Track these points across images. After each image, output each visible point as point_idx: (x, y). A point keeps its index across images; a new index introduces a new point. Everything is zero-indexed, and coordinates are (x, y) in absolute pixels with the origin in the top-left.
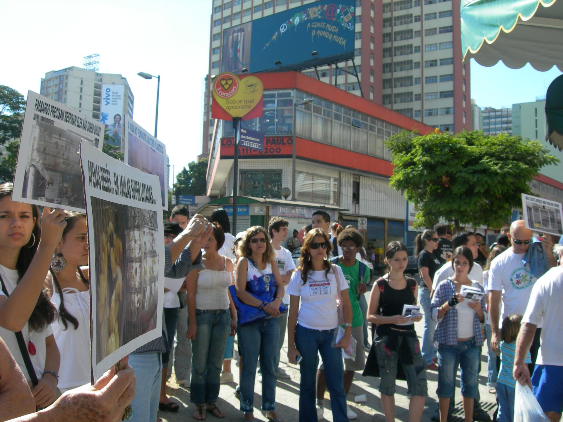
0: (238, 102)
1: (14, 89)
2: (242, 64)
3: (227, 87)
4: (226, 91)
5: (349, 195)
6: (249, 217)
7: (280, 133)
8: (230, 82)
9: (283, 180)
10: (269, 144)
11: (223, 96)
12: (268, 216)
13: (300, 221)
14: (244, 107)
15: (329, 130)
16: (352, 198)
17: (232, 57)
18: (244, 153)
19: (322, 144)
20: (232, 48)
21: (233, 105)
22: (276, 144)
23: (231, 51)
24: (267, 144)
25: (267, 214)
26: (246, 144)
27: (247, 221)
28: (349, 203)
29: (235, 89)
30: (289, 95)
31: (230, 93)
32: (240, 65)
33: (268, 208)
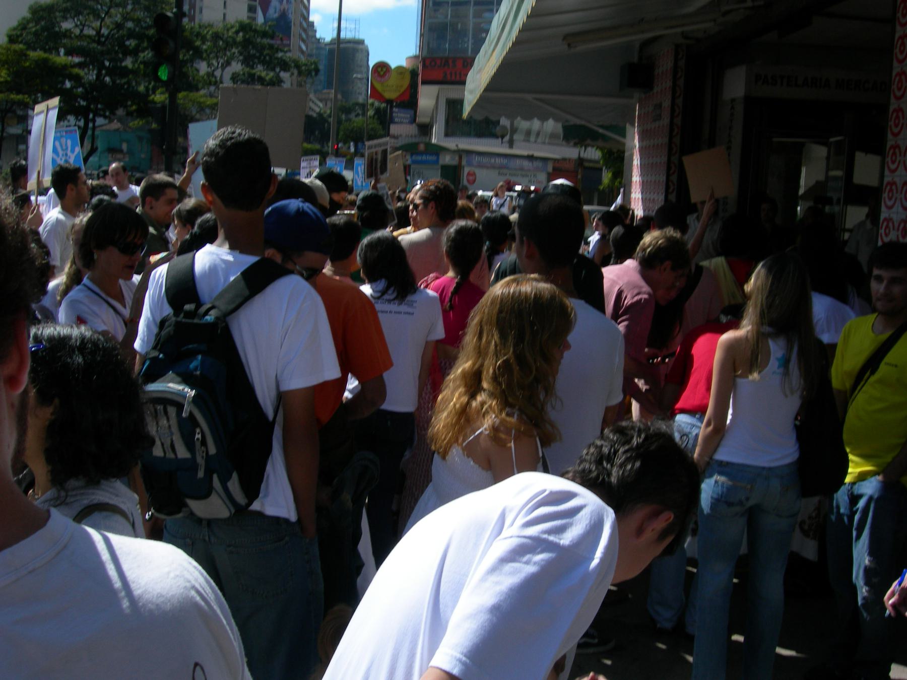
3: (382, 73)
6: (439, 167)
8: (384, 70)
33: (460, 158)
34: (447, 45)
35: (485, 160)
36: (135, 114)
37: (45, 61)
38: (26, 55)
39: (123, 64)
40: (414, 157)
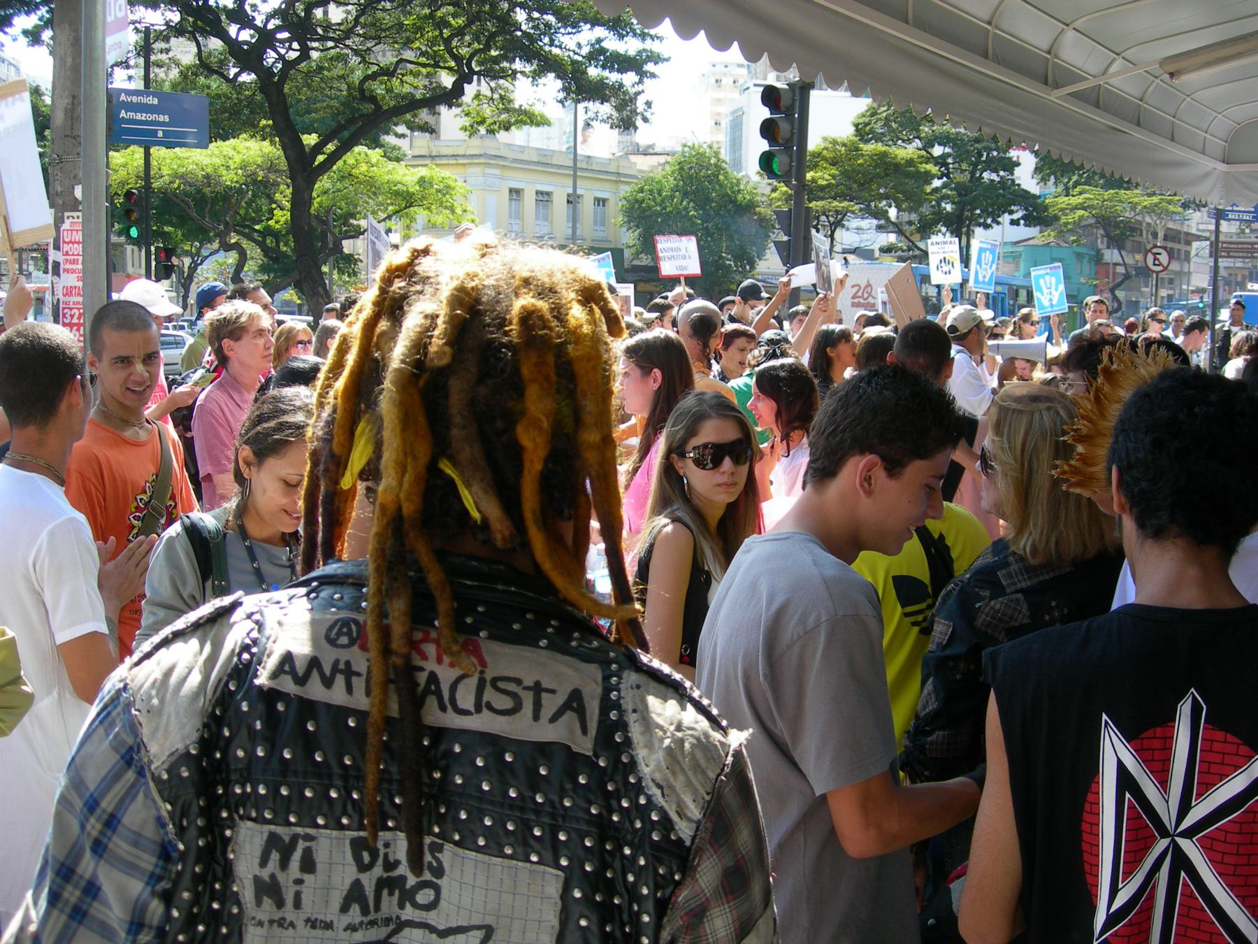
36: (1022, 222)
37: (885, 154)
38: (857, 149)
39: (1008, 155)
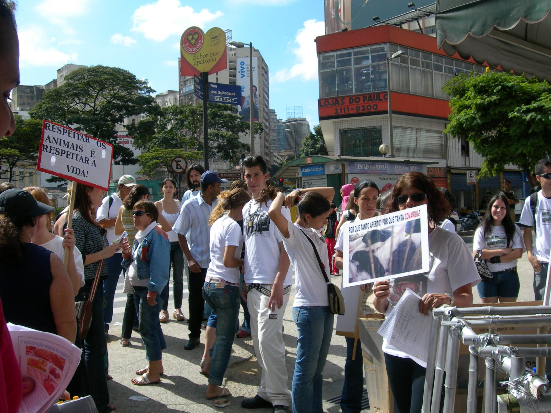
0: (204, 57)
1: (125, 70)
2: (344, 24)
3: (193, 42)
4: (194, 46)
5: (457, 147)
6: (325, 177)
7: (377, 89)
8: (196, 36)
9: (383, 137)
10: (366, 102)
11: (190, 52)
12: (344, 174)
13: (382, 177)
14: (210, 60)
15: (429, 82)
16: (460, 151)
17: (334, 18)
18: (345, 112)
19: (422, 96)
20: (333, 8)
21: (200, 60)
22: (372, 101)
23: (332, 12)
24: (364, 101)
25: (343, 171)
26: (230, 101)
27: (324, 180)
28: (457, 156)
29: (201, 43)
30: (382, 50)
31: (197, 48)
32: (342, 25)
33: (343, 166)
34: (337, 89)
35: (366, 167)
36: (121, 163)
40: (304, 171)
